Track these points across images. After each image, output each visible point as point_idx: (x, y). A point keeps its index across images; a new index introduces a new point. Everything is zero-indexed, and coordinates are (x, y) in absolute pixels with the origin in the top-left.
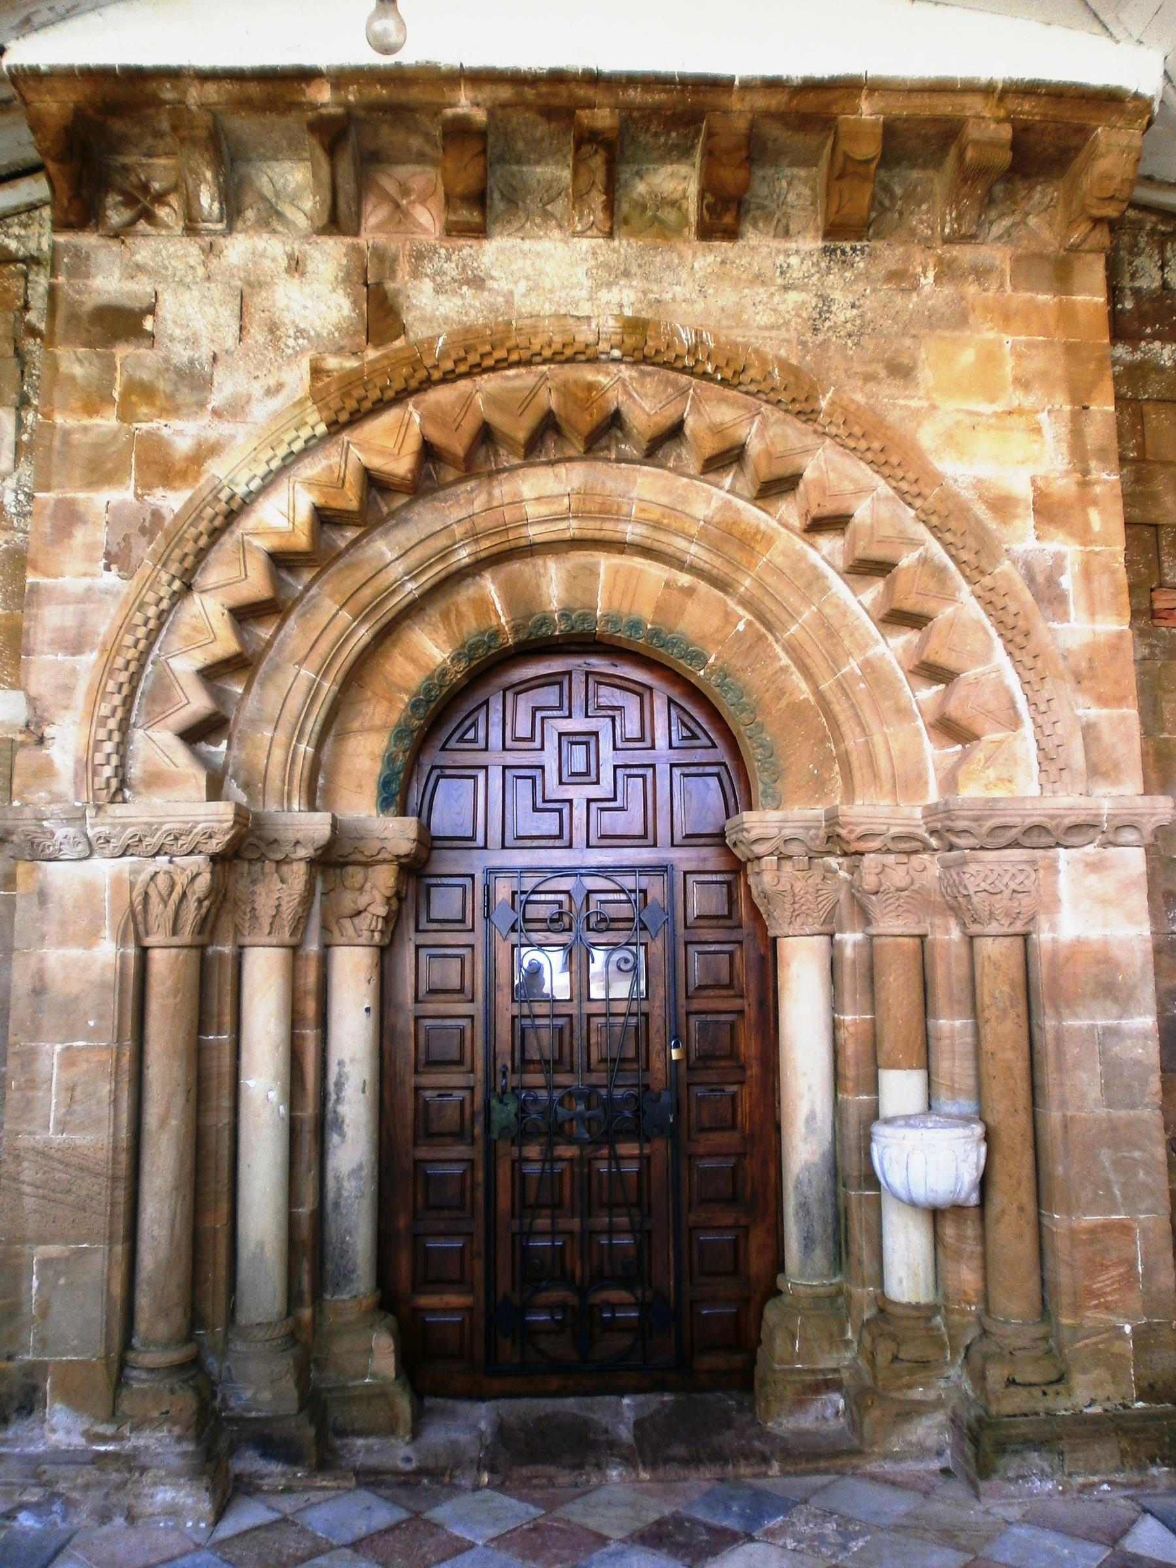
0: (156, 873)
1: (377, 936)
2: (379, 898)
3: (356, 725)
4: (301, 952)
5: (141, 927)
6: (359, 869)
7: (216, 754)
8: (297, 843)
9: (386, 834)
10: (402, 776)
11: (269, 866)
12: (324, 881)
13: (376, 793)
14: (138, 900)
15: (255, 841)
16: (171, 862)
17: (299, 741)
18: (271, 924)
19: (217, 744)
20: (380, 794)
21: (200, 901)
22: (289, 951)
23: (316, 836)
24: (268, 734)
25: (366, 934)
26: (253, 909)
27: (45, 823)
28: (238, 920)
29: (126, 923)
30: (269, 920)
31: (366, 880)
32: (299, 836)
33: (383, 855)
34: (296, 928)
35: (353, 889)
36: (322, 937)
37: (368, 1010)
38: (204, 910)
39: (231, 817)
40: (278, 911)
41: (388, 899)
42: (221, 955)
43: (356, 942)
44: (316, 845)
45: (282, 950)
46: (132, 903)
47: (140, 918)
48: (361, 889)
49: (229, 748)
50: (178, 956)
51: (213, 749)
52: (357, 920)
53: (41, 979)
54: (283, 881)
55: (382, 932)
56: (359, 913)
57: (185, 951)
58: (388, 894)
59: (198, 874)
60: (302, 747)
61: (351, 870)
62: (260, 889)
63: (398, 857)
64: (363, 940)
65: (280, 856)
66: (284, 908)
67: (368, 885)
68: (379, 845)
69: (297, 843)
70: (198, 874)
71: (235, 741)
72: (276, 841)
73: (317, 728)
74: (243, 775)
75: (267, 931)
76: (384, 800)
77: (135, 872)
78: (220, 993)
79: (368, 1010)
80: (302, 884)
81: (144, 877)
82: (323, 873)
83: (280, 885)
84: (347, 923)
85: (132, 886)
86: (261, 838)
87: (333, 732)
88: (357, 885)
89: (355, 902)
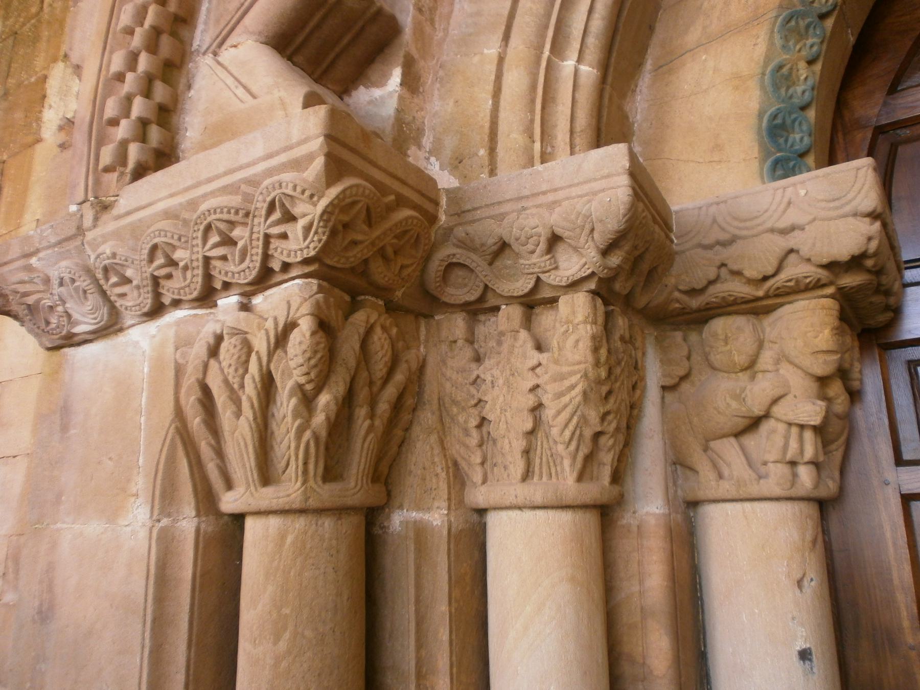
0: (219, 339)
1: (806, 475)
2: (798, 383)
3: (694, 36)
4: (627, 519)
5: (212, 469)
6: (740, 321)
7: (382, 100)
8: (554, 240)
9: (793, 217)
10: (811, 114)
11: (511, 314)
12: (665, 362)
13: (755, 152)
14: (191, 402)
15: (461, 256)
16: (245, 307)
17: (558, 48)
18: (527, 452)
19: (381, 84)
20: (765, 154)
21: (307, 400)
22: (590, 520)
23: (595, 208)
24: (492, 51)
25: (778, 471)
26: (483, 421)
27: (33, 261)
28: (456, 450)
29: (171, 460)
30: (519, 444)
31: (761, 345)
32: (556, 219)
33: (795, 270)
34: (589, 458)
35: (732, 369)
36: (671, 482)
37: (804, 655)
38: (319, 419)
39: (317, 144)
40: (537, 423)
41: (823, 381)
42: (420, 532)
43: (755, 489)
44: (601, 237)
45: (566, 517)
46: (179, 412)
47: (206, 451)
48: (750, 366)
49: (411, 82)
50: (283, 537)
51: (377, 93)
52: (750, 441)
53: (50, 589)
54: (539, 348)
55: (816, 464)
56: (754, 423)
57: (300, 523)
58: (822, 367)
59: (291, 326)
60: (569, 64)
61: (719, 325)
62: (489, 370)
63: (832, 266)
64: (771, 486)
65: (523, 285)
66: (548, 413)
67: (767, 358)
68: (784, 243)
69: (554, 240)
70: (291, 326)
71: (428, 70)
72: (503, 246)
73: (598, 24)
74: (450, 143)
75: (517, 467)
76: (776, 163)
77: (183, 343)
78: (420, 622)
79: (804, 655)
80: (585, 346)
81: (199, 350)
82: (659, 341)
83: (535, 357)
84: (729, 449)
85: (179, 371)
86: (466, 244)
87: (649, 65)
88: (741, 359)
89: (739, 397)
